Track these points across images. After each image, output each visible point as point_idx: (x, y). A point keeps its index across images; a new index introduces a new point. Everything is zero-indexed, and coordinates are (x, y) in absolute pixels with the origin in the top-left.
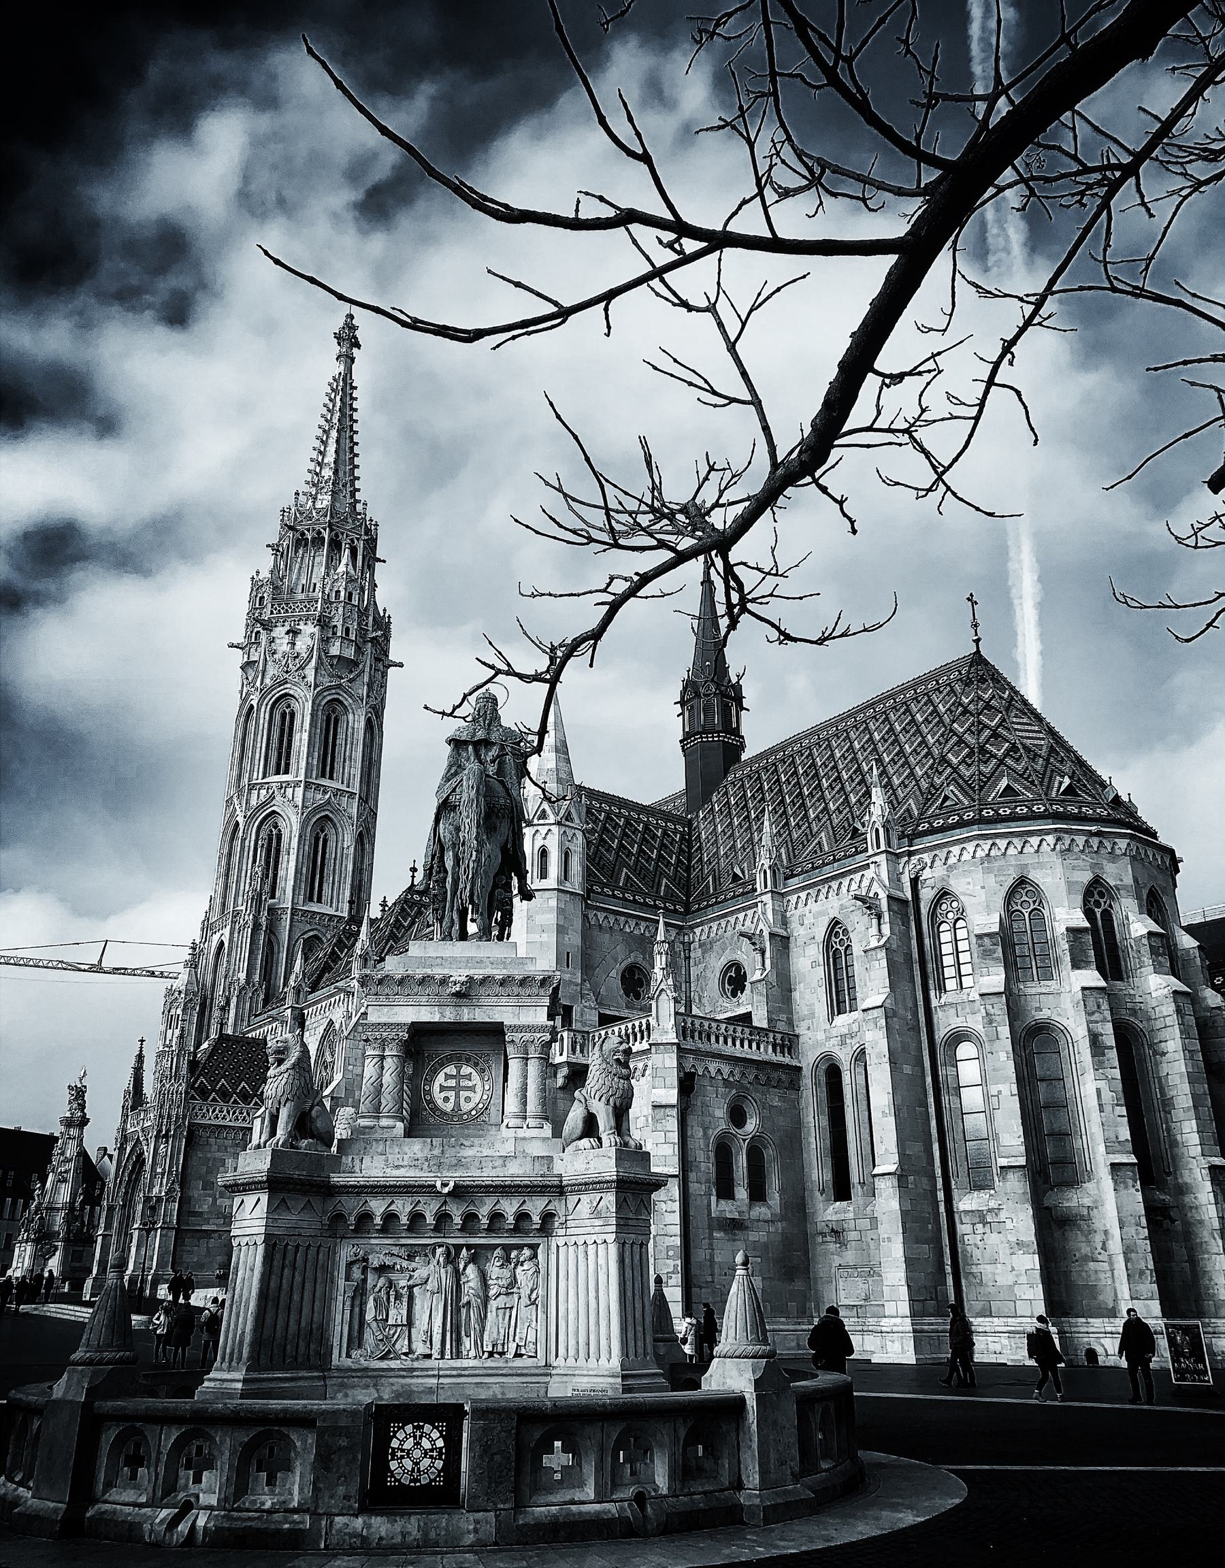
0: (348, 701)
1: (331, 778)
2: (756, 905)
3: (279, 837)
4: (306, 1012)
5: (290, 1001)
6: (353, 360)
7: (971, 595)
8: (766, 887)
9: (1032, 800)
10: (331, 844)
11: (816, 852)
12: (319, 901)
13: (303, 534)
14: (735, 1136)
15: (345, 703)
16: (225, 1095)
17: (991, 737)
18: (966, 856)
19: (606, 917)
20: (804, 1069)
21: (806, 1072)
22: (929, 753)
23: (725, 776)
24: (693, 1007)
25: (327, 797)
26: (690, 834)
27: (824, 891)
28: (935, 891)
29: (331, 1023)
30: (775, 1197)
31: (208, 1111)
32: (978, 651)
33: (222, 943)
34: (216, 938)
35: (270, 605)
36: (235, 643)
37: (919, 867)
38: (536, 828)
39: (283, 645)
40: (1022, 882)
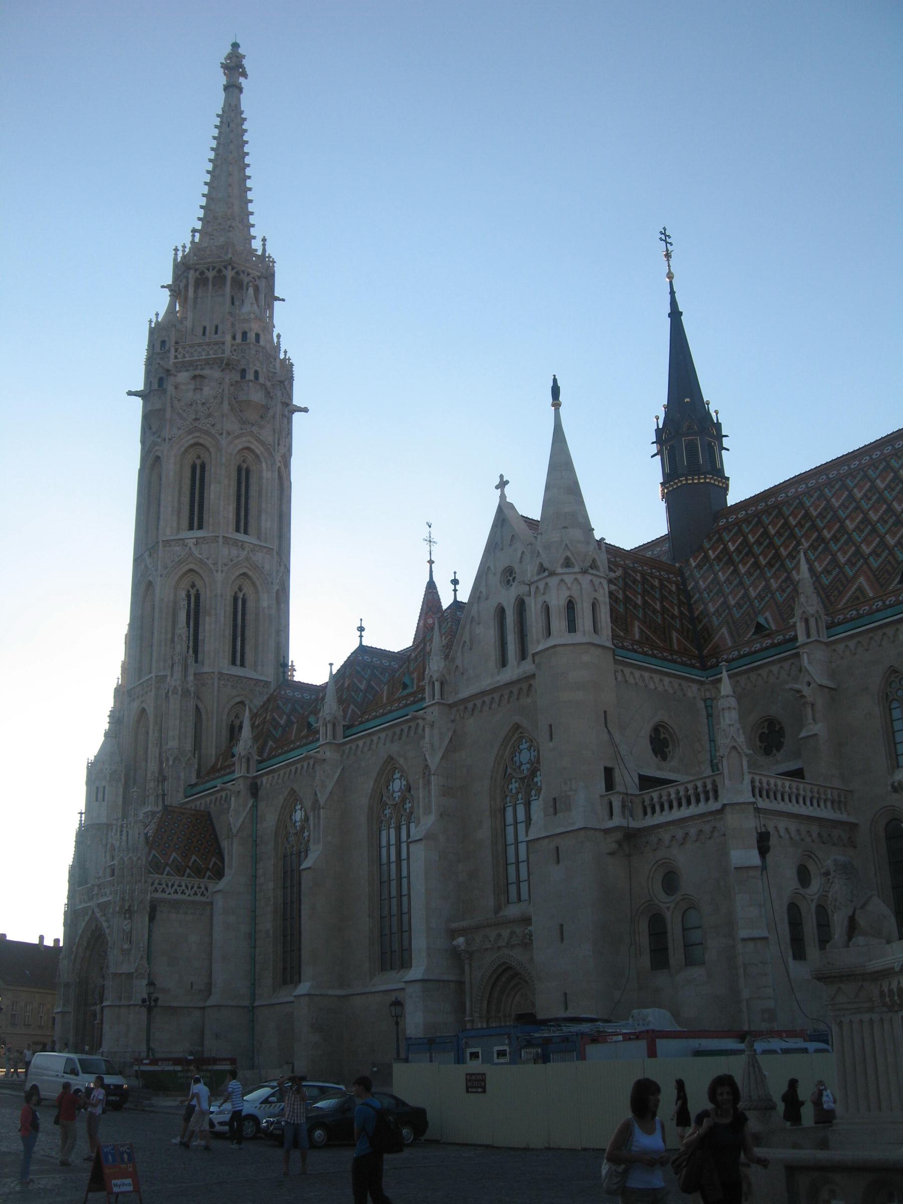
0: (259, 449)
1: (246, 532)
3: (197, 597)
6: (240, 90)
10: (250, 605)
11: (858, 598)
12: (242, 665)
14: (804, 897)
15: (258, 452)
25: (245, 553)
26: (684, 582)
31: (167, 885)
35: (173, 350)
36: (133, 390)
38: (559, 578)
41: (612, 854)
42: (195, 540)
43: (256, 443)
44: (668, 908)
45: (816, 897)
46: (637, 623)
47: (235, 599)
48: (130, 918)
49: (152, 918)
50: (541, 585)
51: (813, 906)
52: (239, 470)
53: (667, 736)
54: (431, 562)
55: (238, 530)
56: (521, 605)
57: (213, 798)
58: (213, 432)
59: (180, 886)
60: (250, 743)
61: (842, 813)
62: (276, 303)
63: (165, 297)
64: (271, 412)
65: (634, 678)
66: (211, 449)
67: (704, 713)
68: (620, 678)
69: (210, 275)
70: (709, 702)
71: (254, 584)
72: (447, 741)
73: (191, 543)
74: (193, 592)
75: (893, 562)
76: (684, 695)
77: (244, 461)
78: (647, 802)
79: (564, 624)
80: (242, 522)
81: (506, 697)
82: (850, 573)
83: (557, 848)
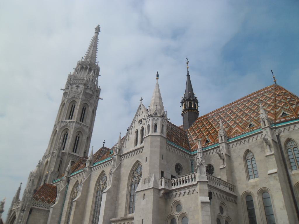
0: (89, 104)
1: (82, 122)
3: (67, 135)
4: (70, 178)
5: (66, 175)
6: (98, 34)
8: (222, 141)
12: (75, 152)
13: (83, 66)
15: (88, 105)
16: (43, 200)
18: (296, 128)
23: (195, 121)
29: (78, 181)
31: (37, 204)
32: (276, 83)
33: (48, 162)
34: (46, 160)
37: (279, 132)
38: (153, 118)
39: (75, 89)
41: (161, 197)
44: (177, 216)
45: (225, 217)
46: (174, 138)
48: (23, 212)
49: (30, 213)
50: (148, 120)
52: (83, 108)
53: (180, 168)
55: (80, 121)
56: (143, 129)
57: (58, 183)
58: (78, 98)
60: (70, 168)
61: (232, 192)
62: (99, 76)
63: (73, 71)
64: (93, 97)
65: (172, 150)
66: (77, 102)
67: (191, 164)
68: (168, 149)
70: (192, 161)
72: (118, 165)
73: (68, 122)
74: (66, 134)
75: (246, 123)
76: (185, 158)
77: (85, 106)
78: (173, 182)
79: (154, 130)
81: (136, 153)
82: (233, 127)
83: (144, 194)
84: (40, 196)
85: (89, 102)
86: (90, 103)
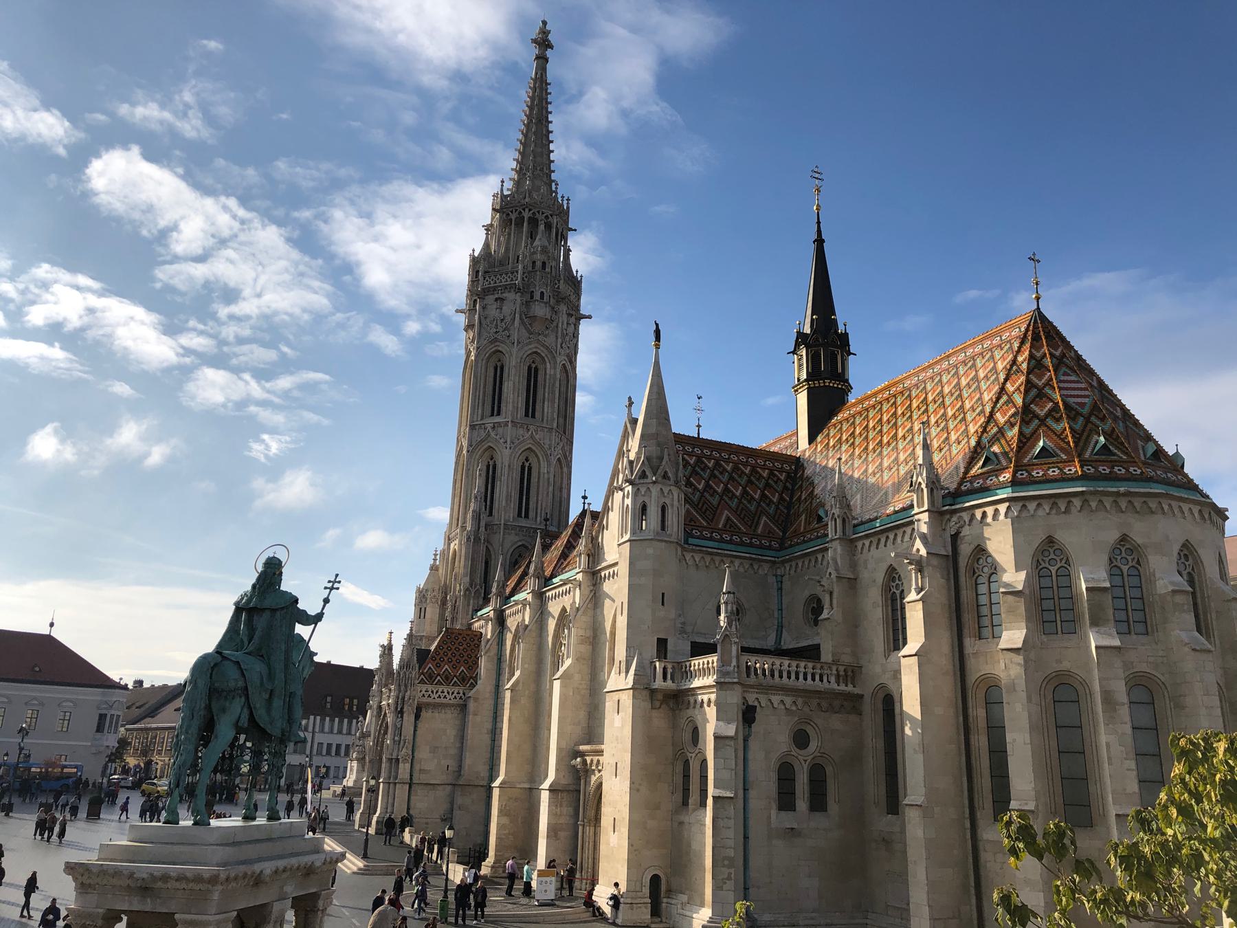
2: (826, 549)
6: (547, 60)
7: (1034, 254)
9: (1065, 462)
12: (527, 516)
17: (1037, 396)
19: (703, 557)
20: (866, 697)
21: (867, 699)
22: (983, 411)
24: (784, 630)
26: (796, 472)
27: (883, 540)
28: (973, 547)
30: (833, 807)
31: (432, 692)
32: (1038, 308)
39: (493, 311)
40: (1050, 540)
42: (492, 425)
43: (542, 348)
47: (523, 467)
49: (417, 717)
51: (805, 767)
52: (530, 368)
54: (699, 426)
59: (443, 692)
69: (513, 216)
70: (779, 579)
71: (537, 456)
73: (489, 427)
77: (533, 362)
80: (530, 409)
84: (438, 666)
85: (543, 345)
86: (547, 348)
